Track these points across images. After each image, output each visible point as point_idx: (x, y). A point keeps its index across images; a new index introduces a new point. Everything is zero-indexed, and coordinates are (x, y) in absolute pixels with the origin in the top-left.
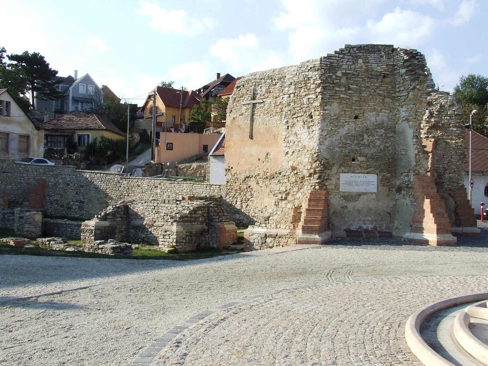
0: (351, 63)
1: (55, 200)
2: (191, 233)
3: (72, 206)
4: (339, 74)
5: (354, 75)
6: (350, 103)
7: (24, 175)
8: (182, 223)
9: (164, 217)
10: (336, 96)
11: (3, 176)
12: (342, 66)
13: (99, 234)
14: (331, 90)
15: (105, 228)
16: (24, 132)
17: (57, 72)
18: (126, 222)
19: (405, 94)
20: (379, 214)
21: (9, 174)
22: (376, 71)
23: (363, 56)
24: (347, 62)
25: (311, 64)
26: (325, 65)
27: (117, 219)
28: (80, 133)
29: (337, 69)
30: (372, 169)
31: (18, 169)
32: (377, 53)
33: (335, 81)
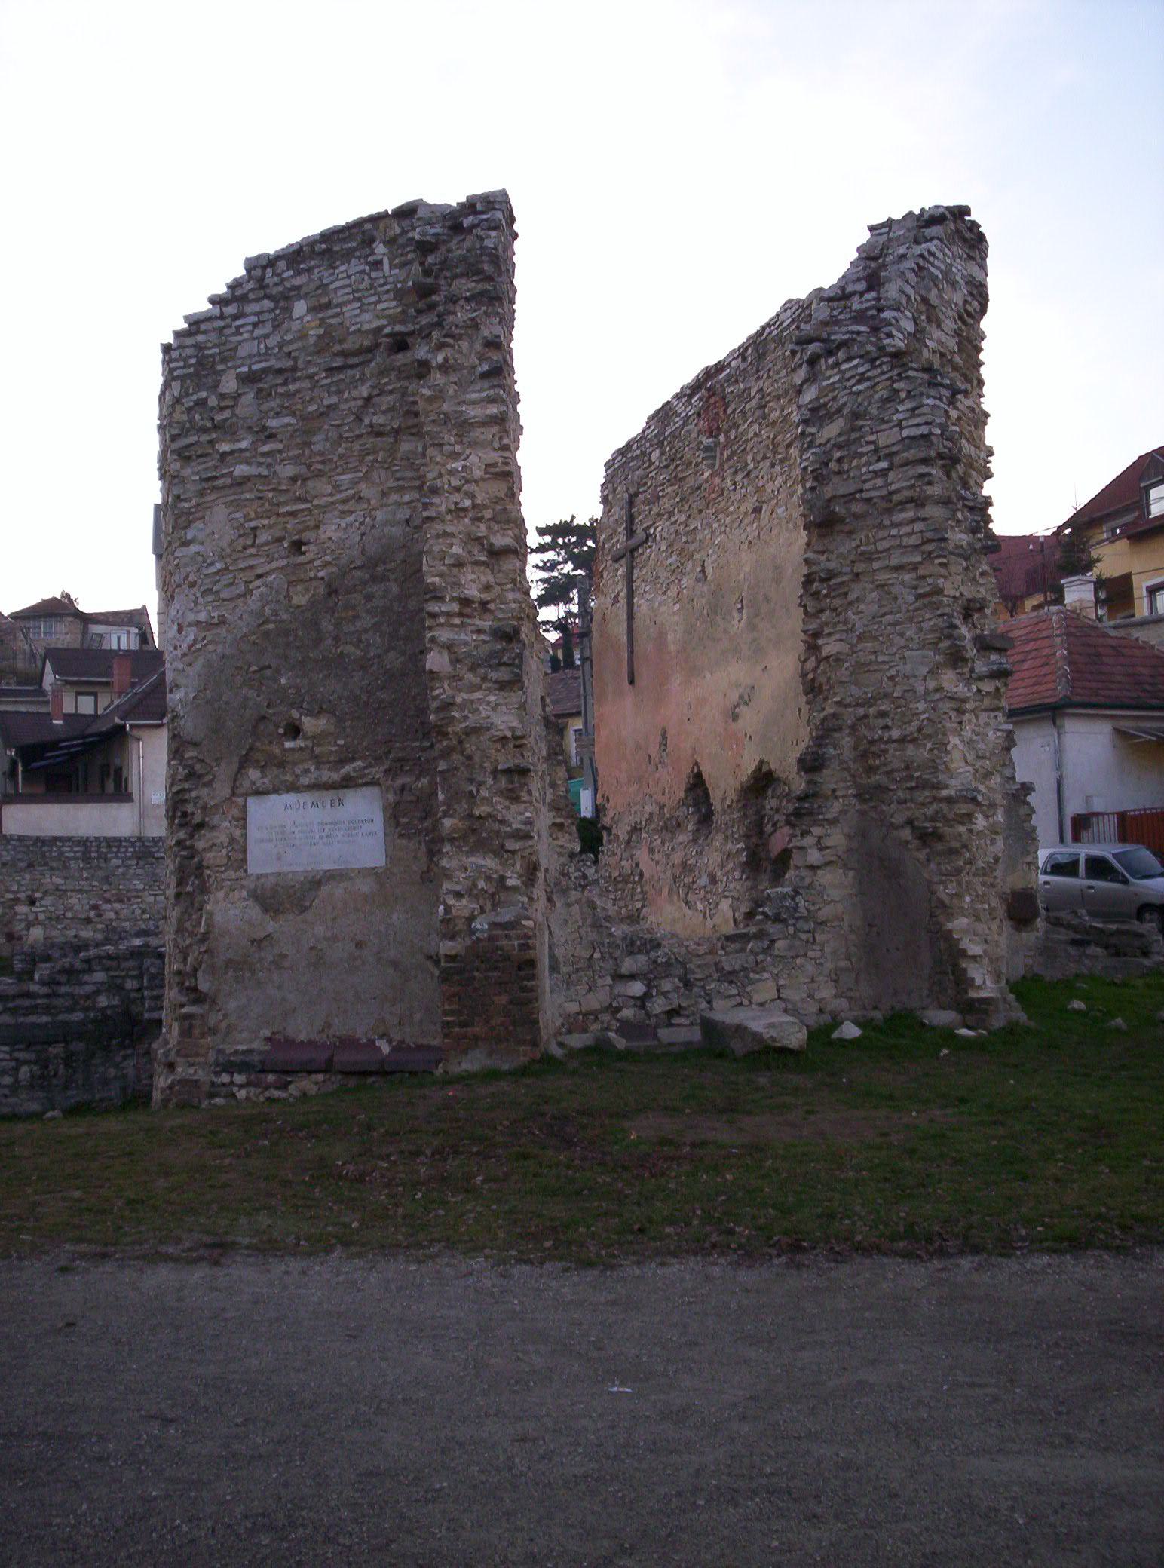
0: (267, 329)
4: (229, 384)
5: (280, 371)
6: (271, 495)
10: (223, 476)
12: (236, 349)
14: (207, 455)
20: (395, 964)
22: (359, 330)
23: (308, 283)
24: (255, 325)
26: (181, 364)
29: (220, 367)
30: (358, 763)
32: (358, 253)
33: (218, 418)
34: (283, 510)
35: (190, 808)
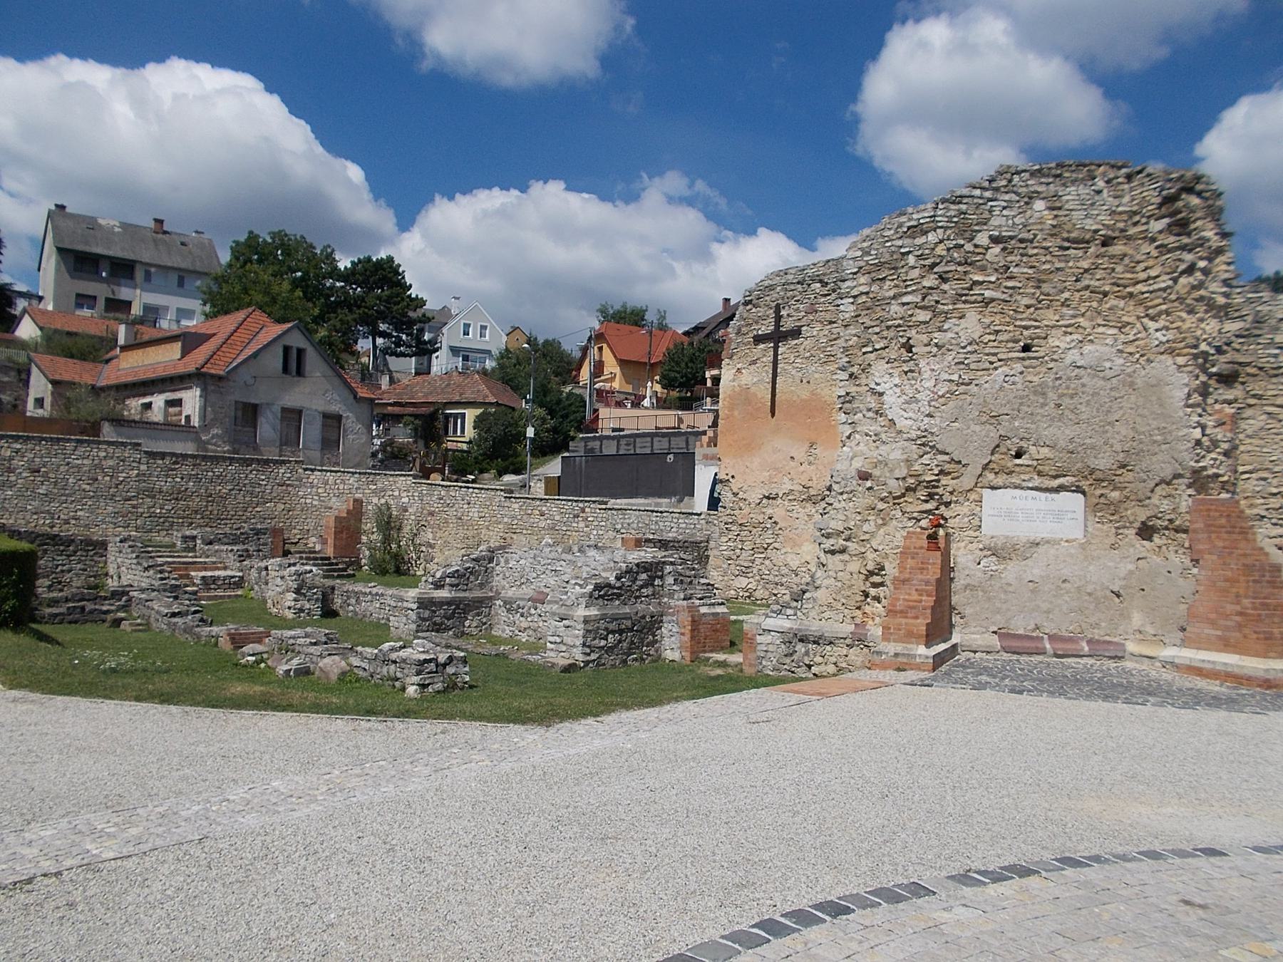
4: (982, 239)
5: (1021, 241)
12: (989, 219)
16: (335, 408)
19: (1163, 285)
24: (1004, 208)
25: (910, 220)
29: (977, 228)
34: (1018, 323)
35: (940, 491)
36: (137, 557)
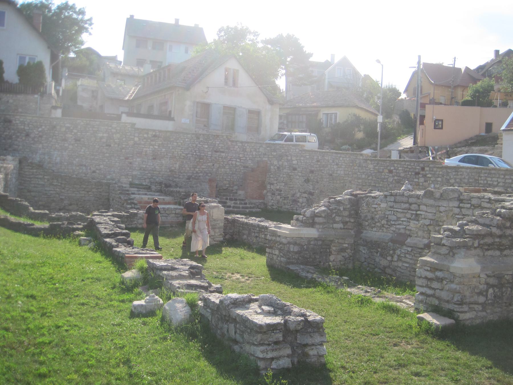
1: (277, 190)
2: (500, 277)
3: (299, 198)
7: (241, 156)
8: (478, 251)
9: (431, 228)
11: (215, 156)
13: (296, 253)
15: (309, 244)
17: (311, 55)
18: (352, 232)
21: (223, 154)
27: (335, 226)
28: (326, 111)
31: (234, 147)
36: (121, 193)
